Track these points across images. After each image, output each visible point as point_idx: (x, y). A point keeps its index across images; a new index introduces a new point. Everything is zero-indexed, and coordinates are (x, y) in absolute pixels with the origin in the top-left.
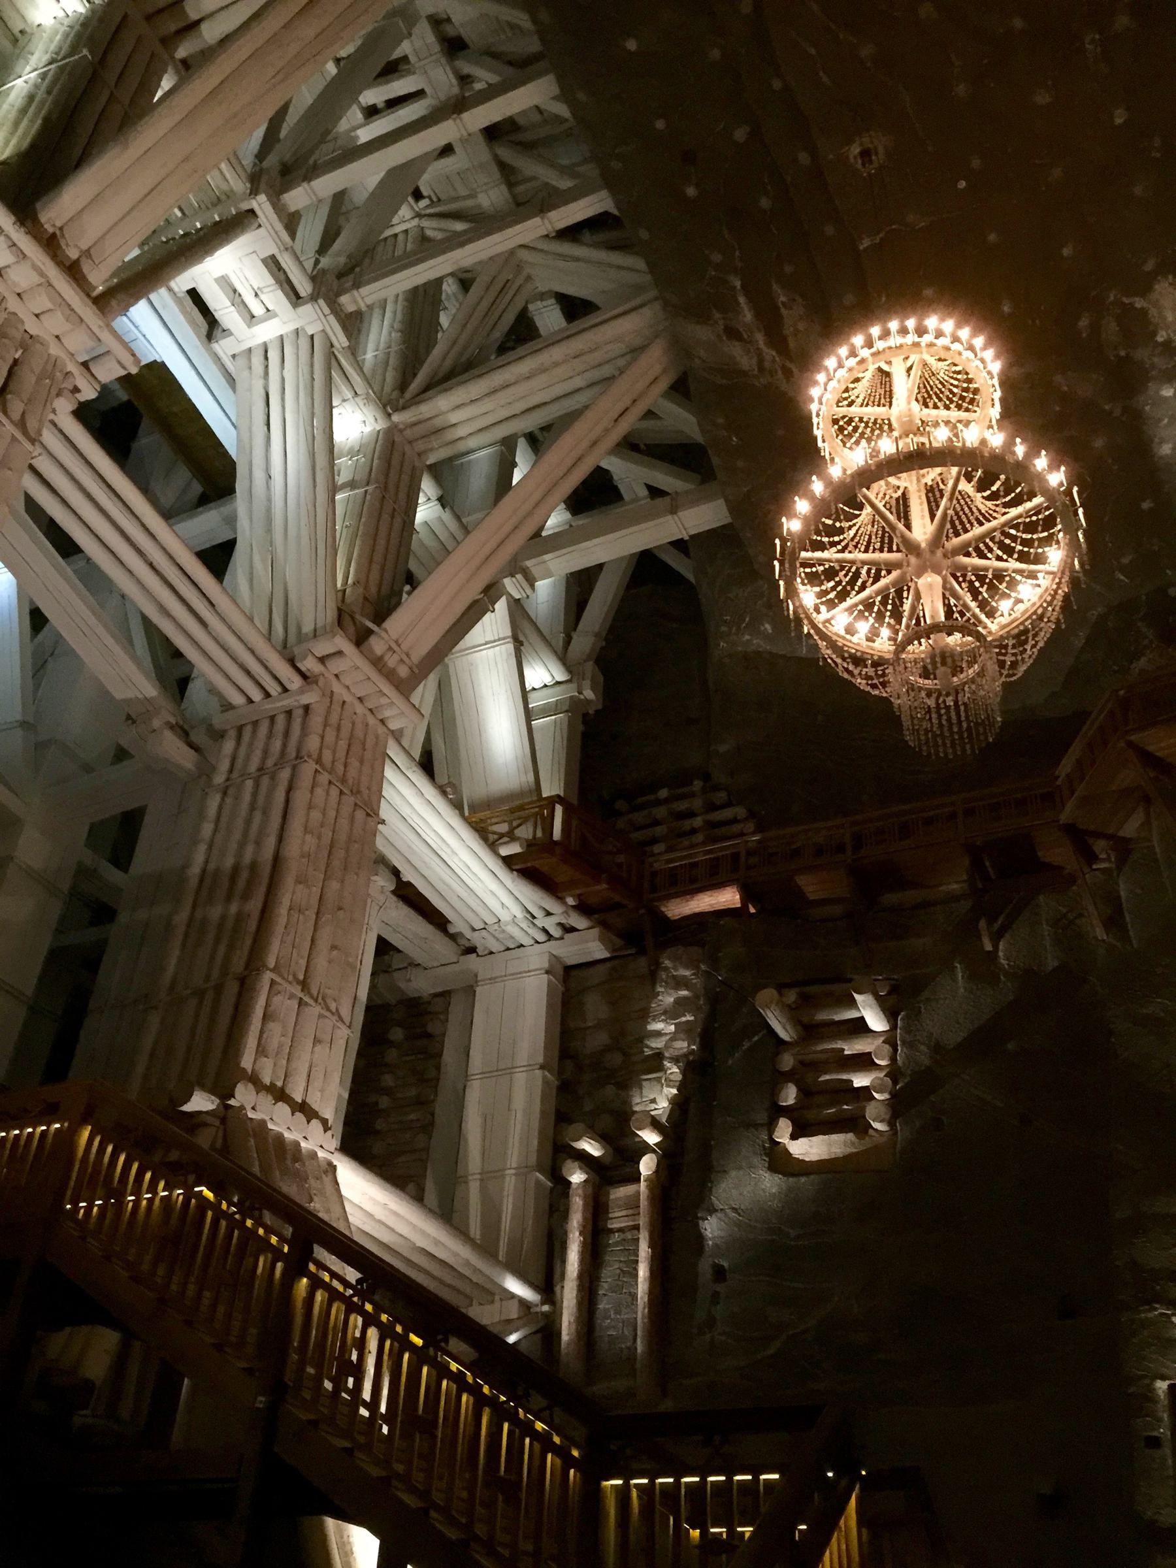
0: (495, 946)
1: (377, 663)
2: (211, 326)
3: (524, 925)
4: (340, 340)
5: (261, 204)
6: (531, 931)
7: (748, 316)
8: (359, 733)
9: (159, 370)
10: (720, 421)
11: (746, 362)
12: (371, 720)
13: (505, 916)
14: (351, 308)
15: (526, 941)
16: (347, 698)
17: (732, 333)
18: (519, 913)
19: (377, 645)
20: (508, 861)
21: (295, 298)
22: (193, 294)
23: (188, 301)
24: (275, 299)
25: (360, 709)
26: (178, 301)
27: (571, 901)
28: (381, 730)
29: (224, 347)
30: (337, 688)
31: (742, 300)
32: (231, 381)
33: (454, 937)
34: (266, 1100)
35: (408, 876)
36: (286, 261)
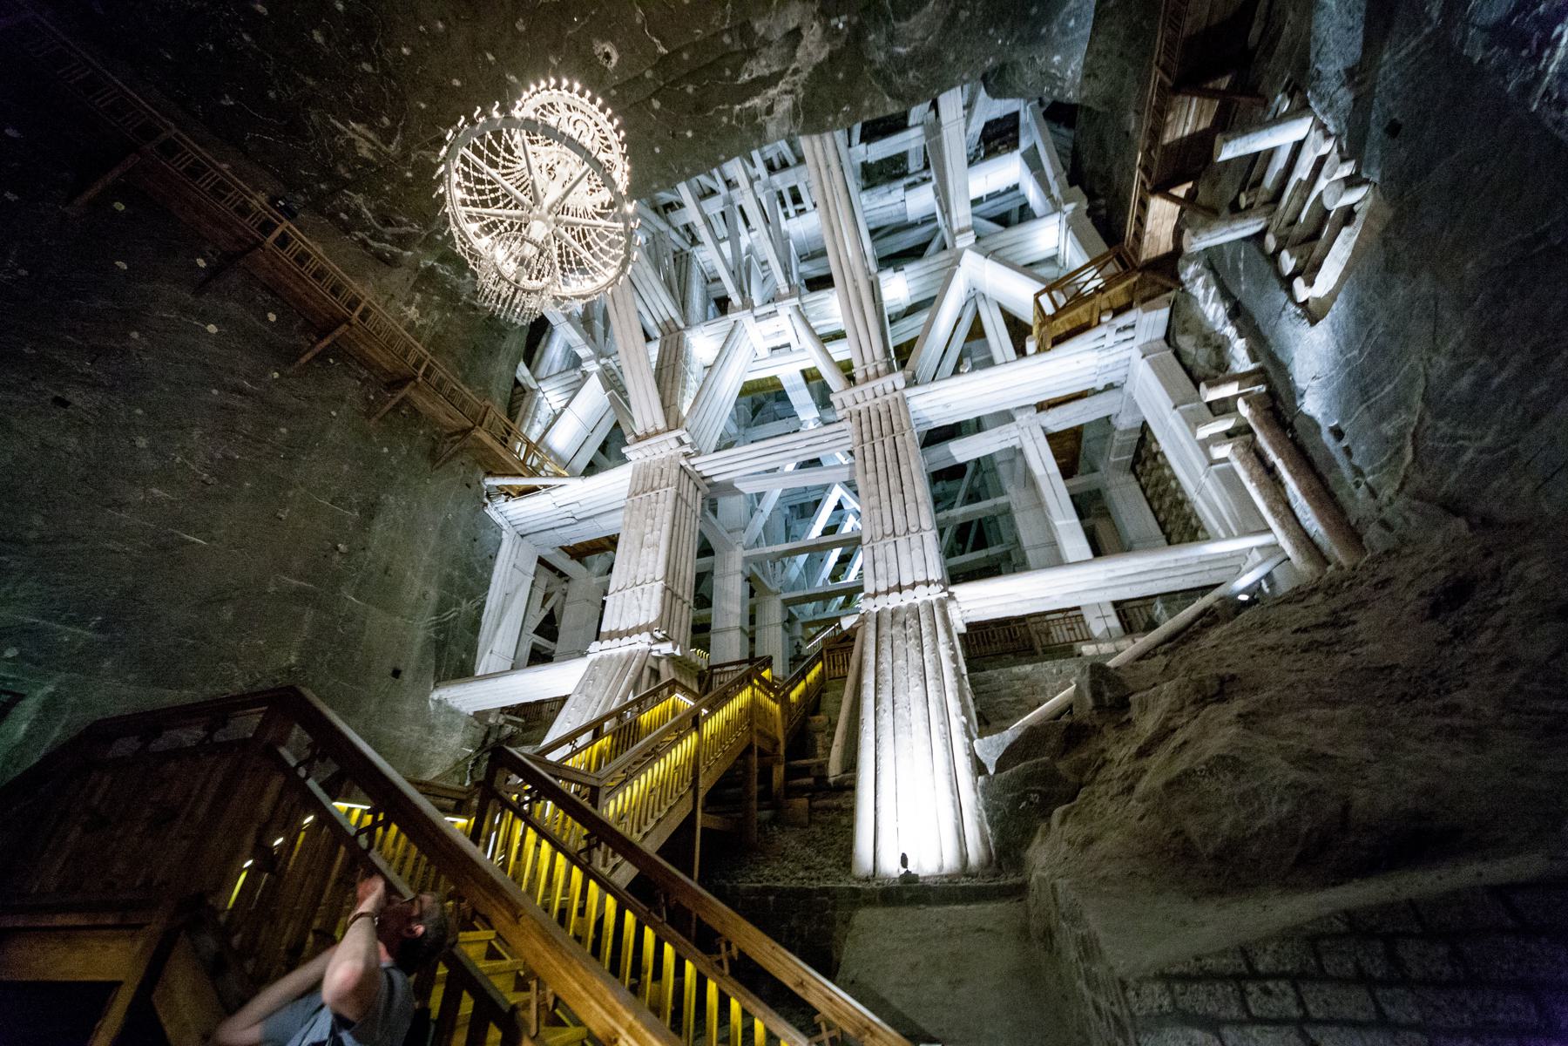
0: (1122, 372)
1: (867, 379)
2: (788, 345)
3: (1105, 353)
4: (795, 301)
5: (732, 317)
6: (1114, 351)
7: (756, 101)
8: (882, 409)
9: (803, 372)
10: (830, 119)
11: (786, 103)
12: (887, 397)
13: (1095, 362)
14: (787, 290)
15: (1125, 355)
16: (867, 404)
17: (770, 111)
18: (1096, 353)
19: (859, 375)
20: (1040, 350)
21: (774, 313)
22: (773, 349)
23: (776, 352)
24: (773, 321)
25: (877, 401)
26: (772, 356)
27: (1104, 319)
28: (896, 394)
29: (794, 346)
30: (859, 407)
31: (747, 105)
32: (803, 350)
33: (1110, 387)
34: (895, 595)
35: (1035, 401)
36: (757, 312)
